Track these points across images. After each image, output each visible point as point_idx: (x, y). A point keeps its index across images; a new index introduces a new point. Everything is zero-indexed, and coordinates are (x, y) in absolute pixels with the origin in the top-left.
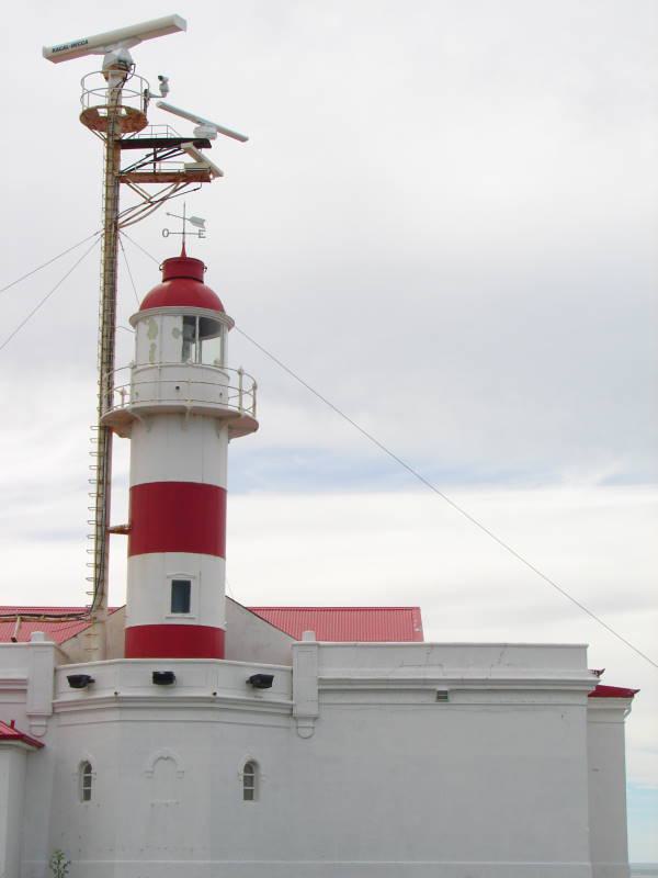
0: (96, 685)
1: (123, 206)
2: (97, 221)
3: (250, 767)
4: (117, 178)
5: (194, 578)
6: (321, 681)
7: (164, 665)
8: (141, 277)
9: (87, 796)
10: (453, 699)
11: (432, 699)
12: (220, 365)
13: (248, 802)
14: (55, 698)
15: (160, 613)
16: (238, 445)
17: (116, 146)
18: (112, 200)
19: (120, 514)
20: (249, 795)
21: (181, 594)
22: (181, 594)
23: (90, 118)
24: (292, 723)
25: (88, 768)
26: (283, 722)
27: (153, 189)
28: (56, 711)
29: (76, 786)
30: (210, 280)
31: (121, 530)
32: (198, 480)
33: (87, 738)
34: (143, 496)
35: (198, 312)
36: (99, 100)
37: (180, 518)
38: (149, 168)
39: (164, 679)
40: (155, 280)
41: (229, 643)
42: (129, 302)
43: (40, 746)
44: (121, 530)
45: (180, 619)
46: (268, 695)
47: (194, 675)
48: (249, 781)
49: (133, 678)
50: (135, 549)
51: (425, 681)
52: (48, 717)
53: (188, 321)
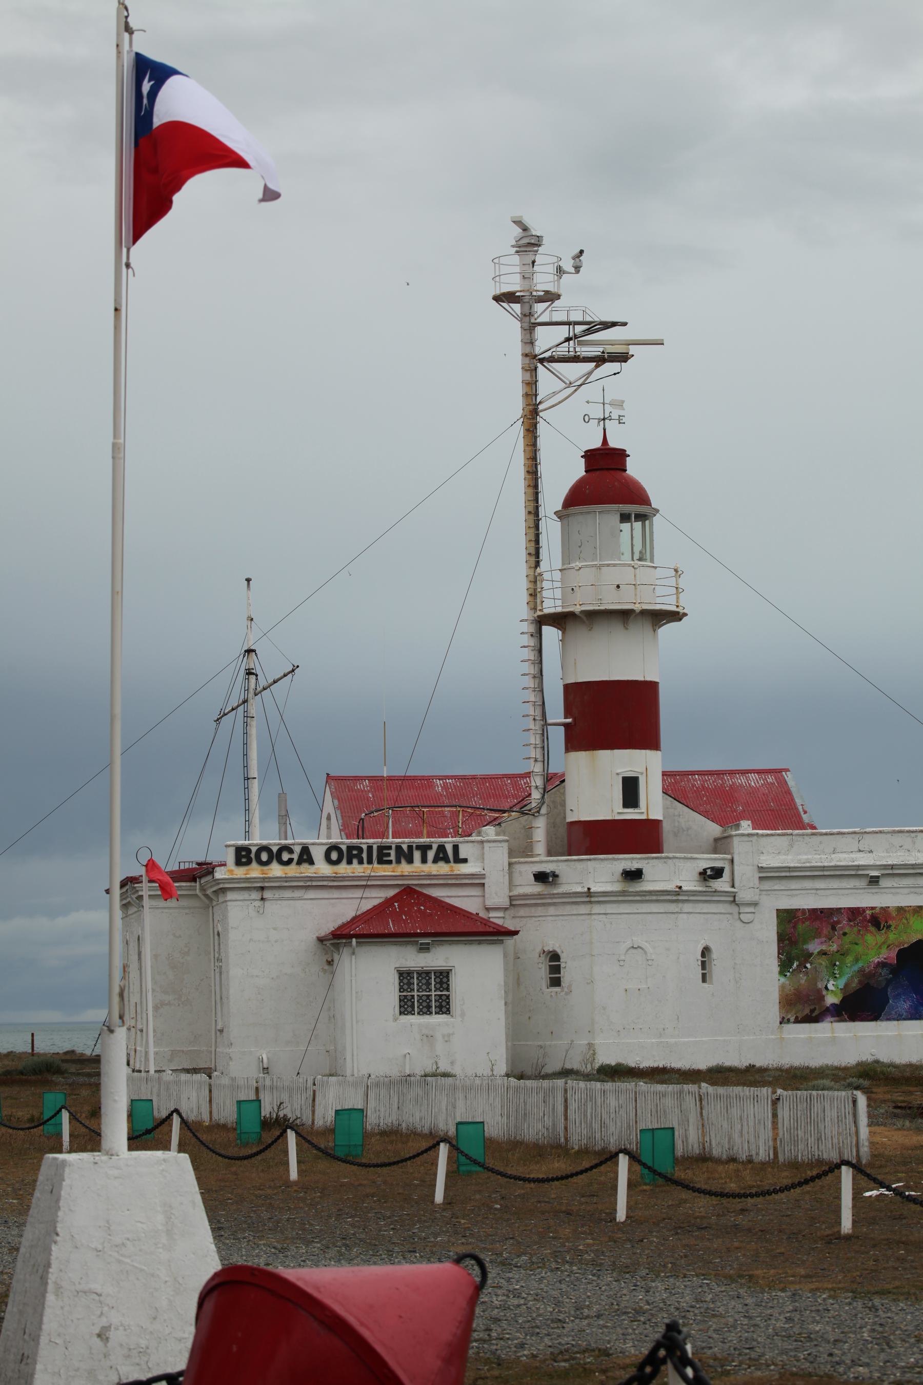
0: (562, 879)
1: (542, 393)
2: (517, 407)
3: (706, 952)
4: (534, 361)
5: (642, 774)
6: (761, 869)
7: (631, 861)
8: (563, 471)
10: (884, 883)
11: (863, 883)
13: (705, 985)
14: (510, 891)
15: (609, 807)
17: (530, 327)
18: (531, 385)
20: (704, 980)
21: (630, 790)
22: (630, 790)
24: (734, 909)
25: (554, 957)
28: (514, 902)
29: (542, 972)
30: (634, 469)
32: (641, 678)
36: (513, 284)
38: (563, 350)
39: (634, 875)
40: (578, 470)
42: (554, 495)
45: (631, 814)
46: (722, 885)
49: (601, 872)
51: (858, 867)
52: (506, 909)
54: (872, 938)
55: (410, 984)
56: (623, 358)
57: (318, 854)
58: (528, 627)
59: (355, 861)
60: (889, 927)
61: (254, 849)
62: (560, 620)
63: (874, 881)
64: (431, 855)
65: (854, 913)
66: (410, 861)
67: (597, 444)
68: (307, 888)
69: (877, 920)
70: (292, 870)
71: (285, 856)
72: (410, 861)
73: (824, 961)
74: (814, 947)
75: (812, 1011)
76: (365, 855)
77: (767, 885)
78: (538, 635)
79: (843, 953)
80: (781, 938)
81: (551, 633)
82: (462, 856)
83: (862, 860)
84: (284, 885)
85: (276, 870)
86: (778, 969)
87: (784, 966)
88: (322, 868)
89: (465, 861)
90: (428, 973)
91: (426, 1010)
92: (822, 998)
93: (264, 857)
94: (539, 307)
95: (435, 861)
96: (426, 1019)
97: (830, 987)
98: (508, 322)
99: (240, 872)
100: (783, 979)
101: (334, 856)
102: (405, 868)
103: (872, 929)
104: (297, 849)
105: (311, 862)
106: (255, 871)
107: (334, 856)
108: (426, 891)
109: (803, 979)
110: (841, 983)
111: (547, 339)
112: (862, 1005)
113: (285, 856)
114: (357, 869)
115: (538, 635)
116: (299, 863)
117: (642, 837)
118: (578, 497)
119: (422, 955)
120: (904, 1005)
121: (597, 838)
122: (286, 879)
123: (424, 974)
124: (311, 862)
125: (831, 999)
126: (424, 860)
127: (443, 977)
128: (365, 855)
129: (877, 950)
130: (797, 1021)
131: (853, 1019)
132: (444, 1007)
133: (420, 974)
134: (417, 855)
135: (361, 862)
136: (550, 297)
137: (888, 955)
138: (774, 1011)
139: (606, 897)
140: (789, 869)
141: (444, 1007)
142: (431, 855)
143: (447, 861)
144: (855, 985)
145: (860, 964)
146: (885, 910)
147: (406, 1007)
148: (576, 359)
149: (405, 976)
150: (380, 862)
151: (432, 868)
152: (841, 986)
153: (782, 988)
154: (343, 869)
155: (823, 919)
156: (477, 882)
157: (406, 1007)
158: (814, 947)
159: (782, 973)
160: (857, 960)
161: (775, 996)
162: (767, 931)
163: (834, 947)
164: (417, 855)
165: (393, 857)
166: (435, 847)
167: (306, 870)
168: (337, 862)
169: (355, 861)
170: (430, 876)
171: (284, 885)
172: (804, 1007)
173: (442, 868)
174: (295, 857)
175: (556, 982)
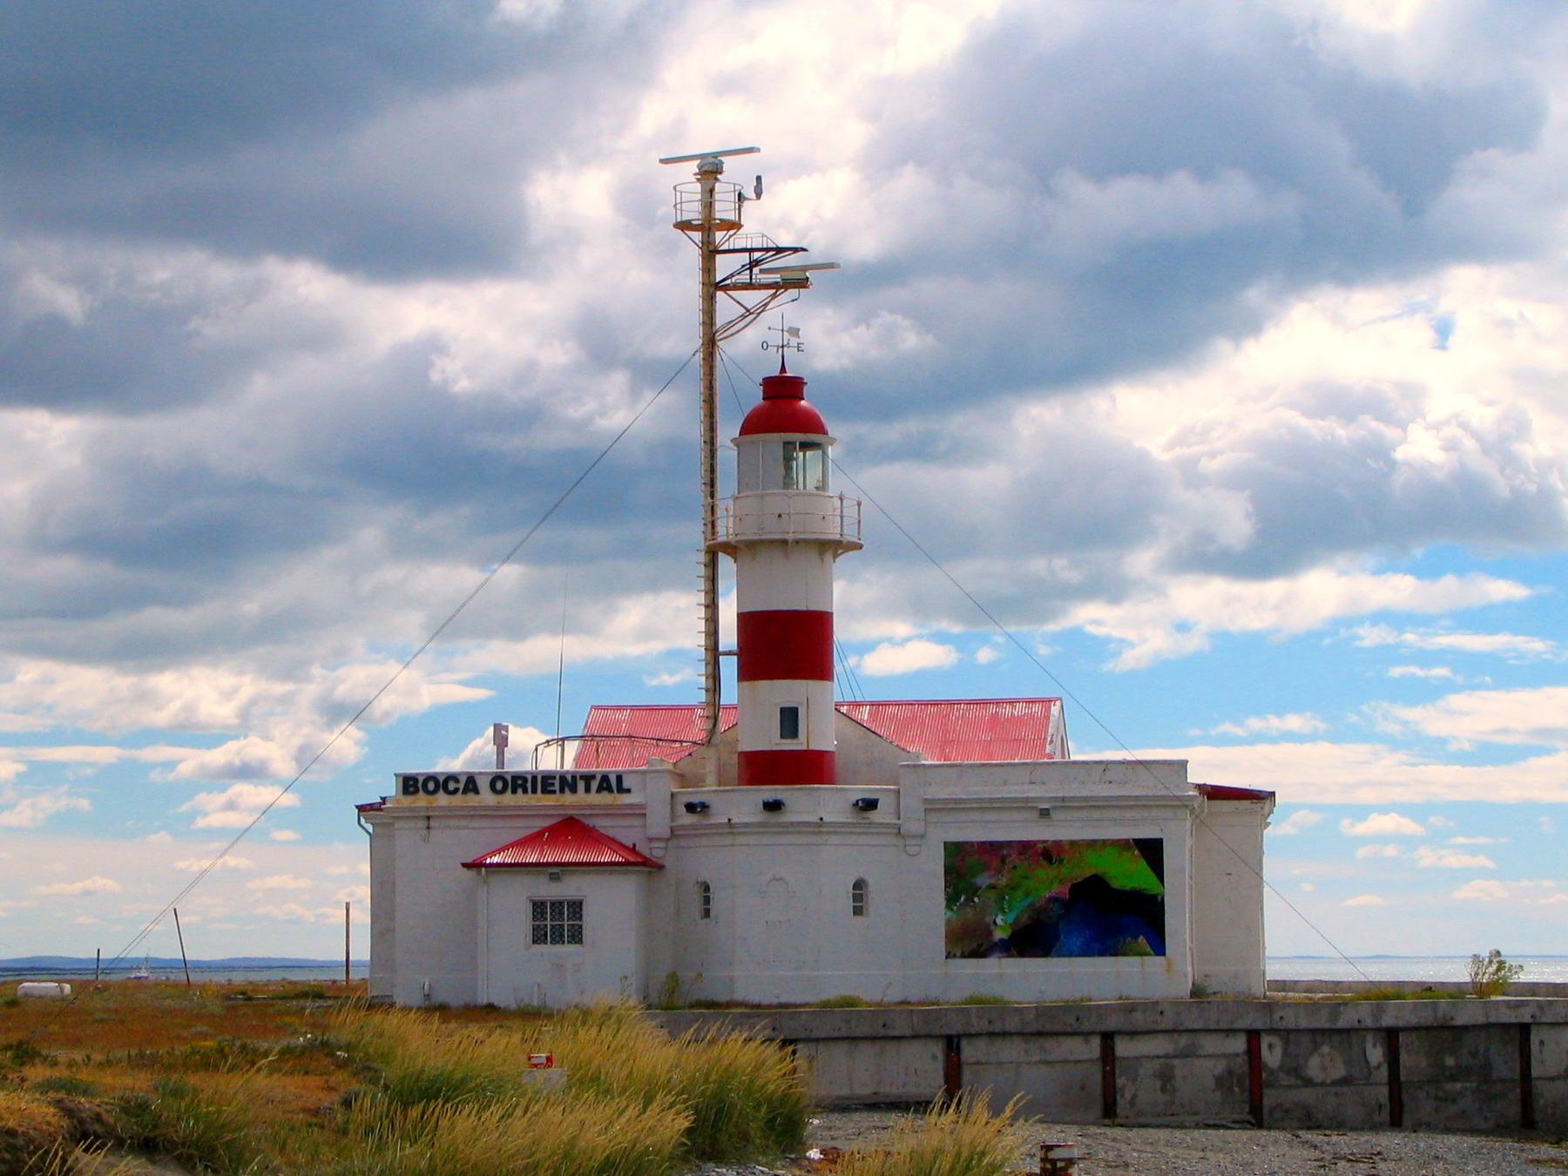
0: (713, 810)
1: (720, 321)
3: (859, 885)
4: (712, 287)
9: (707, 913)
10: (1055, 815)
11: (1035, 815)
12: (822, 486)
13: (859, 918)
15: (768, 738)
16: (845, 561)
17: (710, 253)
19: (729, 637)
20: (858, 911)
22: (790, 719)
23: (684, 226)
24: (900, 842)
25: (707, 888)
26: (892, 840)
27: (752, 298)
31: (729, 653)
32: (802, 607)
33: (705, 860)
34: (747, 621)
35: (798, 437)
36: (693, 212)
37: (788, 644)
38: (744, 277)
39: (774, 806)
40: (756, 398)
41: (839, 763)
43: (661, 867)
44: (729, 653)
45: (789, 745)
47: (802, 801)
48: (858, 898)
50: (748, 672)
51: (1028, 799)
53: (788, 445)
54: (1043, 872)
55: (543, 913)
56: (802, 283)
57: (484, 784)
58: (702, 557)
59: (520, 791)
60: (1061, 862)
61: (421, 780)
62: (731, 549)
63: (1045, 813)
64: (595, 785)
65: (1025, 847)
66: (574, 790)
67: (776, 373)
68: (1010, 809)
69: (1049, 853)
70: (457, 800)
71: (452, 786)
72: (574, 790)
73: (992, 895)
74: (983, 880)
75: (979, 946)
76: (529, 785)
77: (934, 817)
78: (712, 564)
79: (1013, 888)
80: (948, 871)
81: (726, 564)
82: (626, 785)
83: (1035, 792)
84: (449, 814)
85: (442, 799)
86: (944, 903)
87: (951, 899)
88: (487, 797)
89: (628, 791)
90: (561, 903)
91: (558, 939)
92: (990, 933)
93: (431, 786)
94: (719, 236)
95: (599, 790)
96: (559, 948)
97: (999, 921)
98: (690, 250)
99: (407, 801)
100: (949, 913)
101: (499, 785)
102: (568, 798)
103: (1044, 863)
104: (463, 780)
105: (476, 791)
106: (421, 800)
107: (499, 785)
108: (590, 822)
109: (970, 913)
110: (1011, 918)
111: (725, 266)
112: (1032, 939)
113: (452, 786)
114: (521, 799)
115: (712, 564)
116: (464, 792)
117: (810, 768)
118: (754, 425)
119: (553, 885)
120: (1076, 941)
121: (762, 768)
122: (449, 808)
123: (557, 905)
124: (476, 791)
125: (1000, 934)
126: (588, 790)
127: (576, 907)
128: (529, 785)
129: (1047, 884)
130: (963, 956)
131: (1022, 954)
132: (576, 936)
133: (553, 904)
134: (581, 785)
135: (525, 791)
136: (735, 226)
137: (1059, 889)
138: (941, 945)
139: (838, 828)
140: (957, 801)
141: (576, 936)
142: (595, 785)
143: (610, 790)
144: (1024, 919)
145: (1030, 900)
146: (1058, 844)
147: (539, 937)
148: (749, 286)
149: (538, 908)
150: (543, 791)
151: (595, 798)
152: (1010, 921)
153: (948, 922)
154: (508, 799)
155: (993, 851)
156: (639, 812)
157: (539, 937)
158: (983, 880)
159: (949, 906)
160: (1027, 894)
161: (942, 931)
162: (934, 864)
163: (1004, 881)
164: (581, 785)
165: (557, 787)
166: (599, 778)
167: (471, 800)
168: (434, 792)
169: (520, 791)
170: (591, 807)
171: (449, 814)
172: (970, 941)
173: (605, 798)
174: (461, 786)
175: (707, 913)
